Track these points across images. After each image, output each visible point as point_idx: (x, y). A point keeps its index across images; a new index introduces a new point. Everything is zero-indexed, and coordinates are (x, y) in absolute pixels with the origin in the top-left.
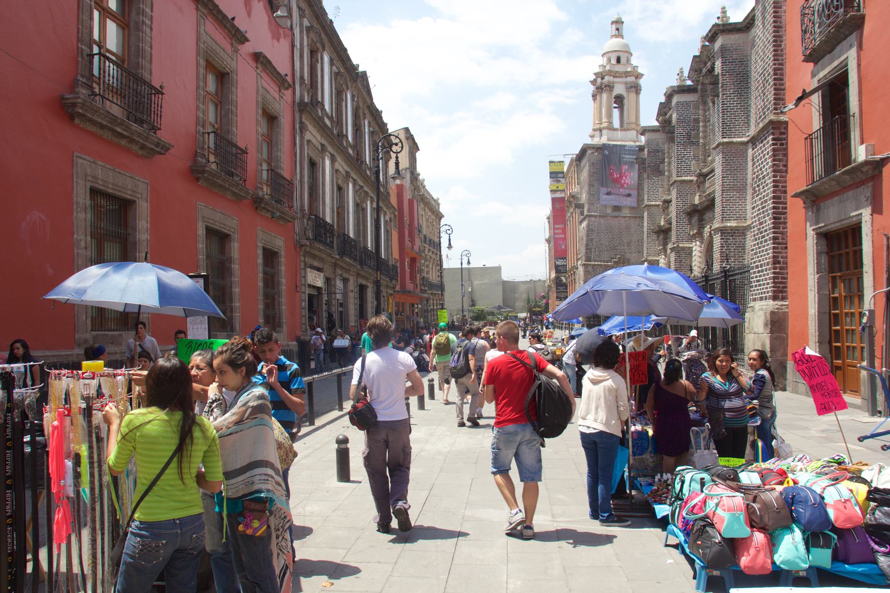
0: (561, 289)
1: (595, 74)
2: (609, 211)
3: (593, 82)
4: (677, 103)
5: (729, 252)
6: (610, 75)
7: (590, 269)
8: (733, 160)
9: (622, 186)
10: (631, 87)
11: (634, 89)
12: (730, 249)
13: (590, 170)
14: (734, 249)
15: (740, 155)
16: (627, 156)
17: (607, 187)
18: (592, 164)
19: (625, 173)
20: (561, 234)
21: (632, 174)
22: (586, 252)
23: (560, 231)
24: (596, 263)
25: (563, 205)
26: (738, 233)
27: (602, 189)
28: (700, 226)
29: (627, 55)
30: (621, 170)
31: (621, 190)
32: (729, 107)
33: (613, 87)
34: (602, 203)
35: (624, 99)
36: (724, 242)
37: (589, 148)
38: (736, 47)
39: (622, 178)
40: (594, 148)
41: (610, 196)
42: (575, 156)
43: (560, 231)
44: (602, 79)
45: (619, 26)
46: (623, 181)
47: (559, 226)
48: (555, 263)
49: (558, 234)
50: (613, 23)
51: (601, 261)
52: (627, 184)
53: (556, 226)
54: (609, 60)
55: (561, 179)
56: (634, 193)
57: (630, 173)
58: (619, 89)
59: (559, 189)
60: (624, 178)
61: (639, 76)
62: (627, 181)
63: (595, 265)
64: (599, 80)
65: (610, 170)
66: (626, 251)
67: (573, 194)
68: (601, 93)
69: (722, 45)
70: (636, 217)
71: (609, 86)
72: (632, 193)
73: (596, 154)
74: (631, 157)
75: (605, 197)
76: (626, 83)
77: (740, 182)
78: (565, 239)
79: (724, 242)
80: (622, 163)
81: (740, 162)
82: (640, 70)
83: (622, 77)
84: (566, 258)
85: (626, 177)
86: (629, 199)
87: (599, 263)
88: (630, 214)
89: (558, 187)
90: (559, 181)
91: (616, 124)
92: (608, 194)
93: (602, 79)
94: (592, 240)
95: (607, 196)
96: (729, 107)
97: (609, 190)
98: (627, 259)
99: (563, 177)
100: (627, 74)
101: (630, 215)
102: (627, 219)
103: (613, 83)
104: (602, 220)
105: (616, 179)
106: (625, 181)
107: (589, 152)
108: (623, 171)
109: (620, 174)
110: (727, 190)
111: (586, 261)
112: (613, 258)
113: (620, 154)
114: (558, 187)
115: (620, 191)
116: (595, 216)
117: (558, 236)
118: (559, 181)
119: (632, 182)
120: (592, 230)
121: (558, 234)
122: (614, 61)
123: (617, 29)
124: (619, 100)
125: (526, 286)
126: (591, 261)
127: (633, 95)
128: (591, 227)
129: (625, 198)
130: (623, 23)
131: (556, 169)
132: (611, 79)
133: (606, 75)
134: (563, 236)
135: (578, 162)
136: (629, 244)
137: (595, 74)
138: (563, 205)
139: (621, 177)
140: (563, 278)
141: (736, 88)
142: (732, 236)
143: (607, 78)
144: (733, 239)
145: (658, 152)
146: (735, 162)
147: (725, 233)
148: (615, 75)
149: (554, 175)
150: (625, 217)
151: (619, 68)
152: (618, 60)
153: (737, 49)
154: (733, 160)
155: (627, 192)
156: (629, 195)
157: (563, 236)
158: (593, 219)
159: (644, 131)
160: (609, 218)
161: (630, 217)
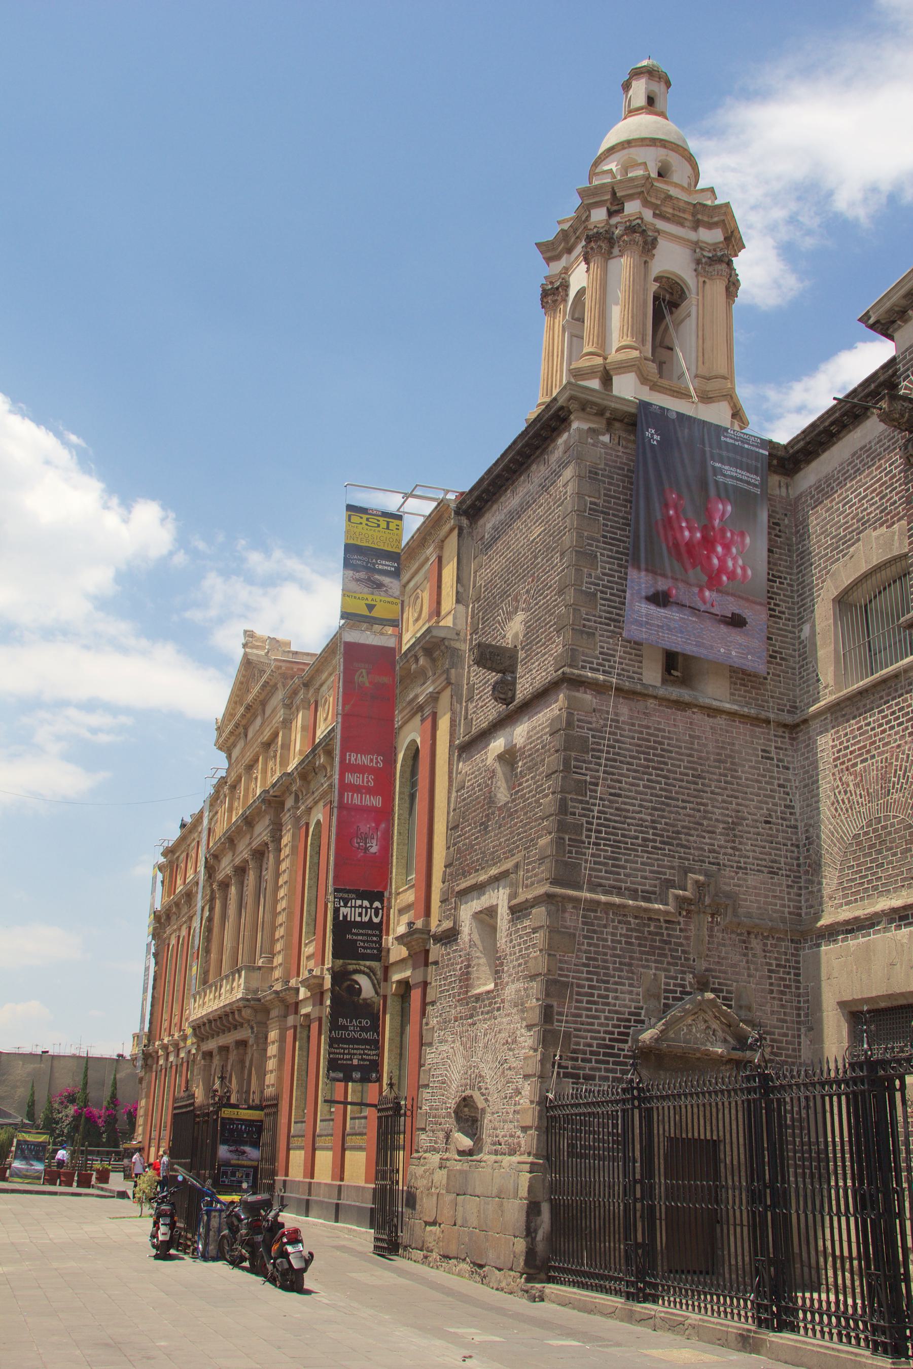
0: (353, 1027)
2: (652, 675)
6: (646, 203)
7: (572, 920)
9: (713, 581)
13: (580, 495)
16: (728, 470)
17: (652, 570)
18: (591, 475)
19: (723, 530)
20: (370, 791)
21: (748, 540)
22: (559, 842)
23: (367, 780)
24: (603, 898)
25: (385, 680)
27: (632, 573)
30: (710, 518)
31: (707, 593)
34: (632, 631)
39: (712, 550)
41: (662, 611)
42: (451, 496)
43: (367, 780)
45: (658, 88)
46: (715, 561)
47: (364, 760)
48: (336, 911)
49: (356, 789)
51: (619, 892)
52: (732, 576)
53: (353, 758)
55: (386, 580)
56: (756, 616)
57: (742, 534)
59: (375, 614)
60: (719, 549)
62: (730, 564)
63: (594, 905)
65: (666, 506)
66: (723, 860)
67: (442, 634)
70: (756, 721)
72: (747, 613)
73: (606, 438)
74: (744, 475)
75: (646, 609)
76: (696, 246)
78: (384, 814)
80: (712, 492)
83: (680, 223)
84: (379, 896)
85: (727, 547)
86: (736, 636)
87: (617, 900)
88: (734, 702)
89: (371, 607)
90: (379, 586)
92: (660, 599)
94: (581, 788)
95: (653, 609)
97: (662, 585)
98: (728, 895)
99: (396, 574)
101: (735, 707)
102: (721, 721)
104: (624, 710)
105: (689, 545)
106: (722, 561)
107: (578, 424)
108: (717, 522)
109: (705, 529)
111: (555, 882)
112: (670, 884)
113: (703, 452)
114: (371, 607)
115: (704, 602)
116: (599, 688)
117: (356, 800)
118: (379, 586)
119: (749, 572)
120: (582, 745)
121: (356, 789)
125: (30, 1067)
126: (578, 887)
128: (577, 732)
129: (723, 629)
131: (375, 537)
133: (630, 197)
134: (376, 801)
135: (465, 522)
137: (583, 193)
138: (385, 680)
139: (708, 542)
140: (364, 982)
143: (632, 208)
149: (356, 559)
150: (713, 712)
155: (731, 606)
156: (736, 622)
157: (376, 801)
158: (587, 697)
160: (651, 703)
161: (732, 714)
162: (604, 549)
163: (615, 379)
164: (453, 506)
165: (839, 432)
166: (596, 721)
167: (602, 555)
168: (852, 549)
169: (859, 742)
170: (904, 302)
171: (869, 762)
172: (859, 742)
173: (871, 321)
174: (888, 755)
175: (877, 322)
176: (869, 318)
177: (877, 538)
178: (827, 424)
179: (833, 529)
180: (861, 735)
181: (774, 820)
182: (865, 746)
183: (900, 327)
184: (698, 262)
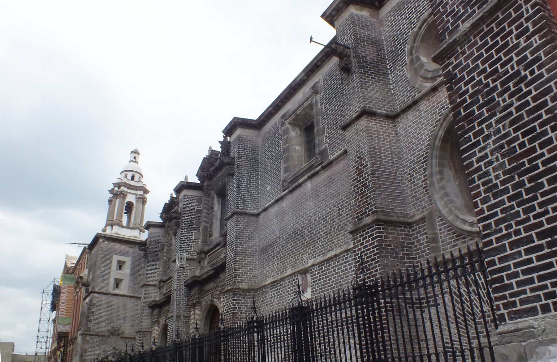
1: (114, 184)
3: (111, 191)
4: (185, 196)
5: (241, 313)
6: (125, 187)
8: (246, 228)
10: (140, 198)
11: (141, 200)
12: (242, 310)
14: (245, 311)
15: (252, 224)
26: (249, 295)
28: (200, 296)
29: (139, 175)
32: (243, 183)
33: (126, 195)
35: (133, 205)
36: (236, 303)
37: (101, 236)
38: (250, 138)
40: (105, 237)
44: (119, 188)
50: (132, 152)
54: (126, 176)
58: (131, 198)
61: (146, 192)
64: (116, 189)
66: (121, 325)
68: (117, 198)
69: (239, 135)
71: (123, 194)
73: (106, 242)
77: (251, 248)
79: (236, 303)
81: (251, 231)
82: (148, 188)
91: (125, 223)
93: (119, 188)
96: (243, 183)
100: (136, 188)
103: (127, 192)
107: (101, 240)
110: (239, 254)
122: (129, 177)
123: (135, 158)
124: (129, 207)
127: (140, 205)
130: (139, 154)
132: (126, 189)
133: (122, 186)
136: (124, 319)
137: (114, 184)
141: (249, 169)
142: (244, 298)
143: (122, 188)
144: (245, 300)
145: (158, 243)
146: (247, 230)
147: (237, 294)
148: (130, 187)
151: (132, 183)
152: (133, 178)
153: (251, 140)
154: (246, 228)
159: (149, 226)
163: (114, 226)
164: (87, 247)
166: (97, 300)
184: (136, 198)
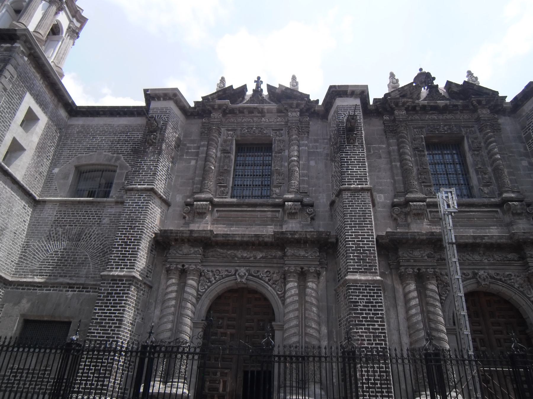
162: (7, 98)
165: (102, 115)
167: (5, 99)
168: (91, 153)
169: (71, 218)
170: (162, 95)
171: (74, 227)
172: (71, 218)
173: (148, 93)
174: (84, 227)
175: (149, 94)
176: (148, 91)
177: (106, 155)
178: (100, 110)
179: (85, 143)
180: (72, 216)
181: (17, 233)
182: (73, 221)
183: (155, 100)
